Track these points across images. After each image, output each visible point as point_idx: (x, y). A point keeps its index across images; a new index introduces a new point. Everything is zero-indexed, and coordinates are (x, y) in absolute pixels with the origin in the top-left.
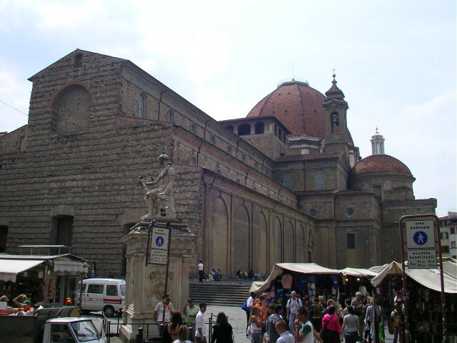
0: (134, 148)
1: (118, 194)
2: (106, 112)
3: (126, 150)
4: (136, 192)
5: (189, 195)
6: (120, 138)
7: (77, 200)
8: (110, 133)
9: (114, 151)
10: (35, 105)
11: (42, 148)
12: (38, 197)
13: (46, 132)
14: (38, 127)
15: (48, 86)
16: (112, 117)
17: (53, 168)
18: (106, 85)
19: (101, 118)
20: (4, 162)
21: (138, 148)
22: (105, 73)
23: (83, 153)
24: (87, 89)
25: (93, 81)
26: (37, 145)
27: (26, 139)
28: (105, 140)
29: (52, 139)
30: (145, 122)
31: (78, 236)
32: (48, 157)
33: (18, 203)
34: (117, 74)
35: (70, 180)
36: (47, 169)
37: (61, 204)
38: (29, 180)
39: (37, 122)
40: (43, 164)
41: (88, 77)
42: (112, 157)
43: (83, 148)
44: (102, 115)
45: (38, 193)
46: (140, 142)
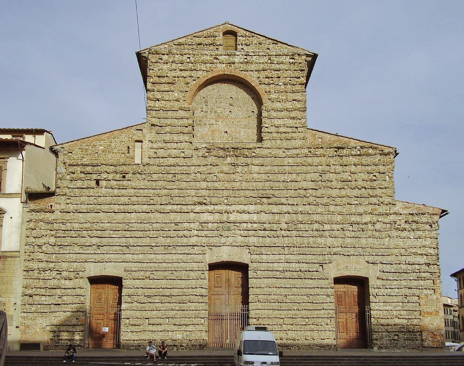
0: (339, 176)
1: (321, 236)
2: (291, 122)
3: (326, 177)
4: (348, 234)
5: (428, 242)
6: (316, 160)
7: (252, 240)
8: (298, 151)
9: (309, 176)
10: (159, 96)
11: (181, 161)
12: (181, 233)
13: (187, 138)
14: (168, 129)
15: (181, 70)
16: (300, 129)
17: (204, 193)
18: (285, 84)
19: (282, 130)
20: (104, 176)
21: (346, 176)
22: (282, 66)
23: (255, 176)
24: (253, 85)
25: (263, 74)
26: (170, 156)
27: (146, 144)
28: (290, 160)
29: (196, 149)
30: (353, 143)
31: (258, 291)
32: (192, 176)
33: (140, 242)
34: (301, 70)
35: (238, 212)
36: (193, 192)
37: (224, 245)
38: (158, 207)
39: (168, 122)
40: (184, 185)
41: (253, 67)
42: (304, 185)
43: (256, 169)
44: (284, 125)
45: (180, 226)
46: (347, 168)
